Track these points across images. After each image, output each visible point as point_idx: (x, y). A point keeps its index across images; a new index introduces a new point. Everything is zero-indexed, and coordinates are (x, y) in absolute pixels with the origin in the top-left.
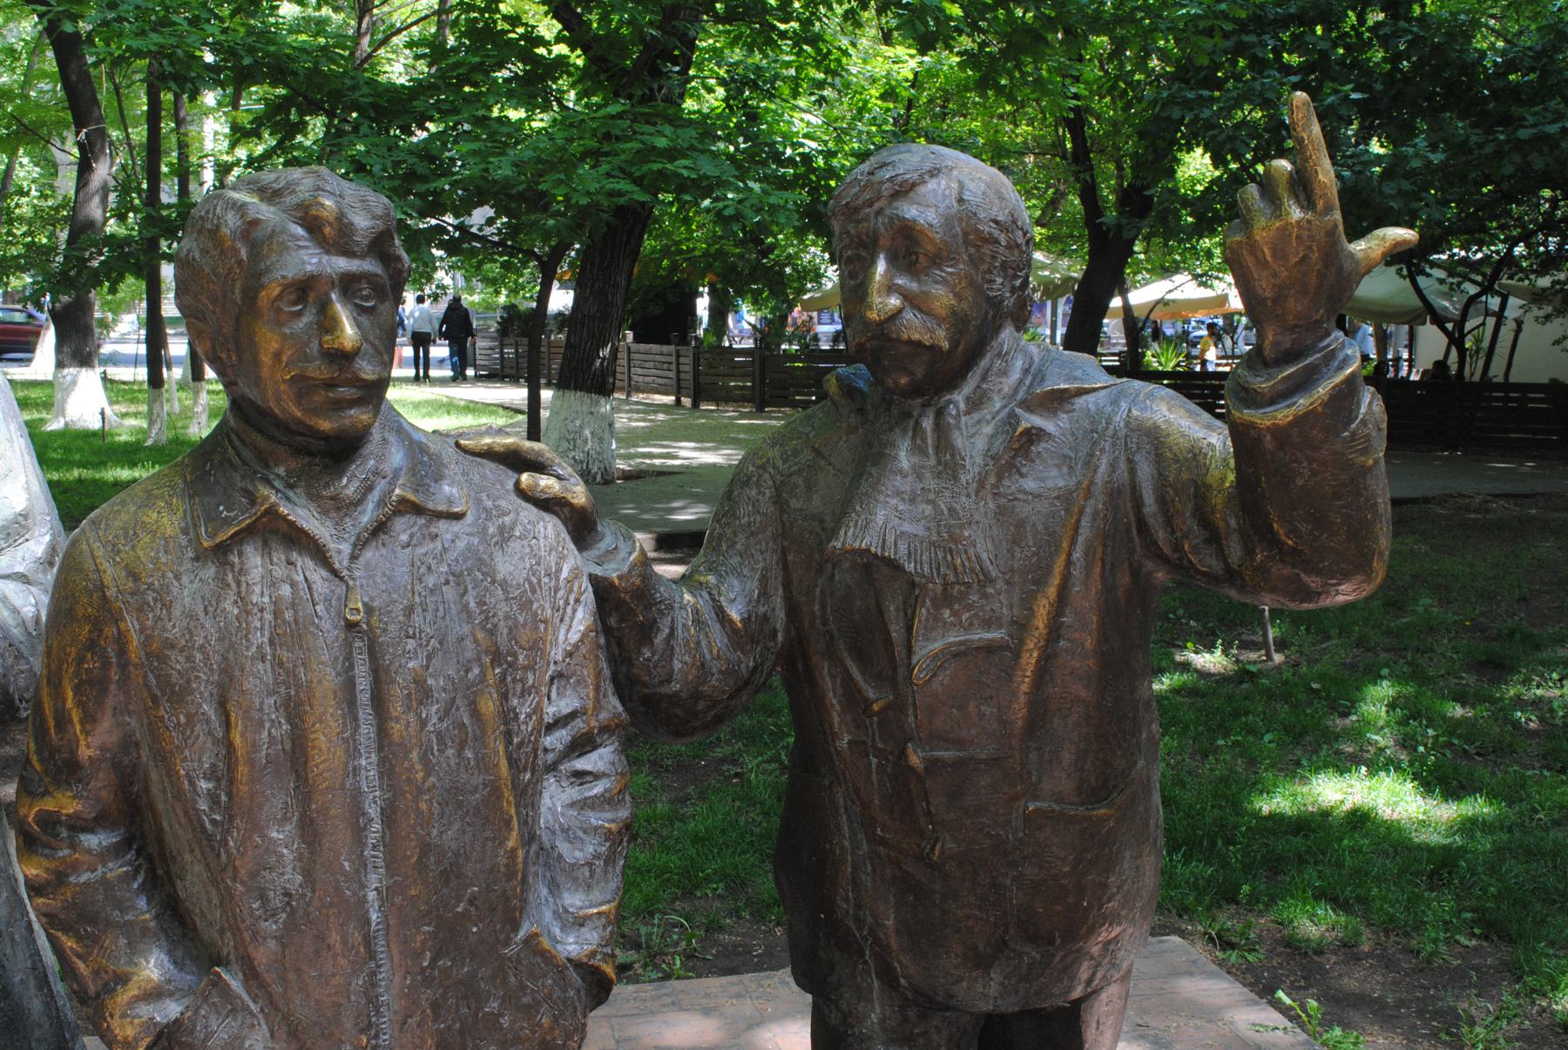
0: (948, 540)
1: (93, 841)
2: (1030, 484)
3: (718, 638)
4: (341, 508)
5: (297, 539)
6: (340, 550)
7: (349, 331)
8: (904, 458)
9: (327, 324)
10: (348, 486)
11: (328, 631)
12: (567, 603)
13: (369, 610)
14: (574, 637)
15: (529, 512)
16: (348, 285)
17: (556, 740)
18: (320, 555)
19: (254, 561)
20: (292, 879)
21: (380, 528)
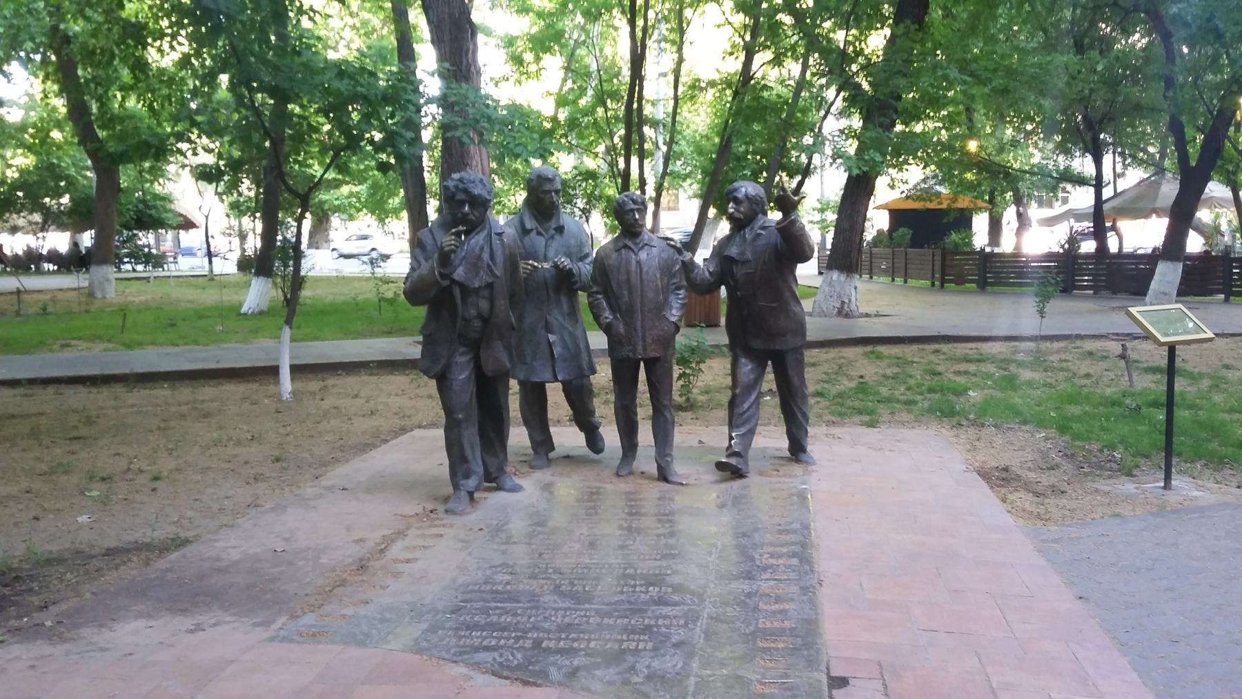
0: (742, 253)
1: (600, 296)
2: (759, 243)
3: (707, 274)
4: (636, 244)
5: (630, 248)
6: (636, 250)
7: (637, 216)
8: (738, 239)
10: (638, 241)
11: (634, 262)
15: (668, 248)
17: (673, 287)
19: (623, 251)
20: (626, 299)
21: (643, 247)
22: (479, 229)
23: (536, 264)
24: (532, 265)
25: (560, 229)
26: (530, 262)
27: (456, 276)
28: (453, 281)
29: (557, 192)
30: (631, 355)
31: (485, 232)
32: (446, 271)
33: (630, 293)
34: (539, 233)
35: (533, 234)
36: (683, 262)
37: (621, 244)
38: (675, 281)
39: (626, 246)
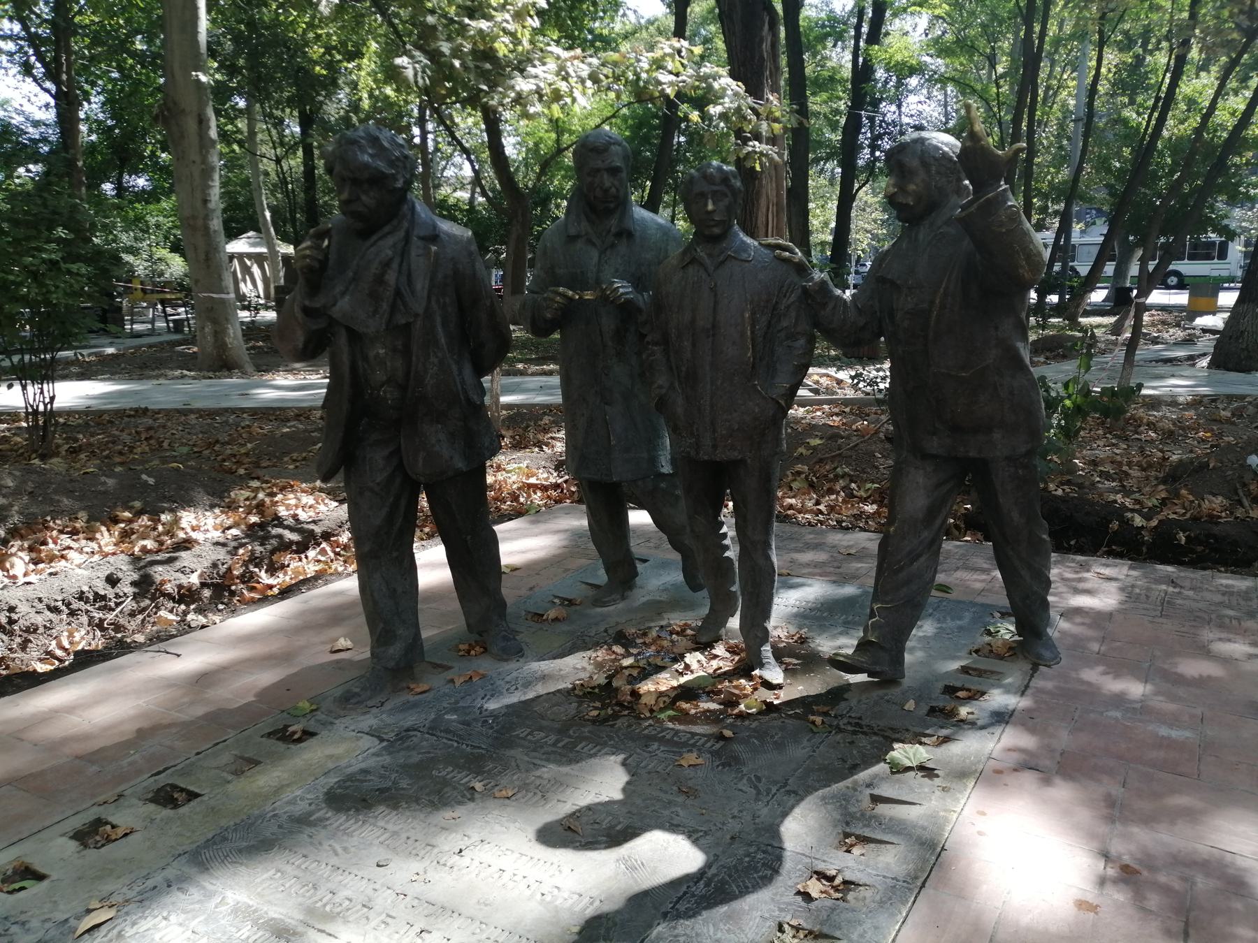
5: (702, 264)
6: (711, 269)
9: (706, 205)
12: (787, 291)
13: (716, 285)
14: (789, 302)
16: (714, 193)
18: (706, 270)
21: (723, 262)
22: (387, 229)
23: (570, 293)
24: (563, 295)
25: (626, 234)
26: (561, 289)
27: (336, 312)
28: (332, 322)
29: (614, 171)
30: (693, 453)
31: (401, 234)
32: (317, 303)
33: (694, 345)
34: (590, 242)
35: (579, 244)
36: (805, 291)
37: (687, 259)
38: (785, 323)
39: (694, 261)
